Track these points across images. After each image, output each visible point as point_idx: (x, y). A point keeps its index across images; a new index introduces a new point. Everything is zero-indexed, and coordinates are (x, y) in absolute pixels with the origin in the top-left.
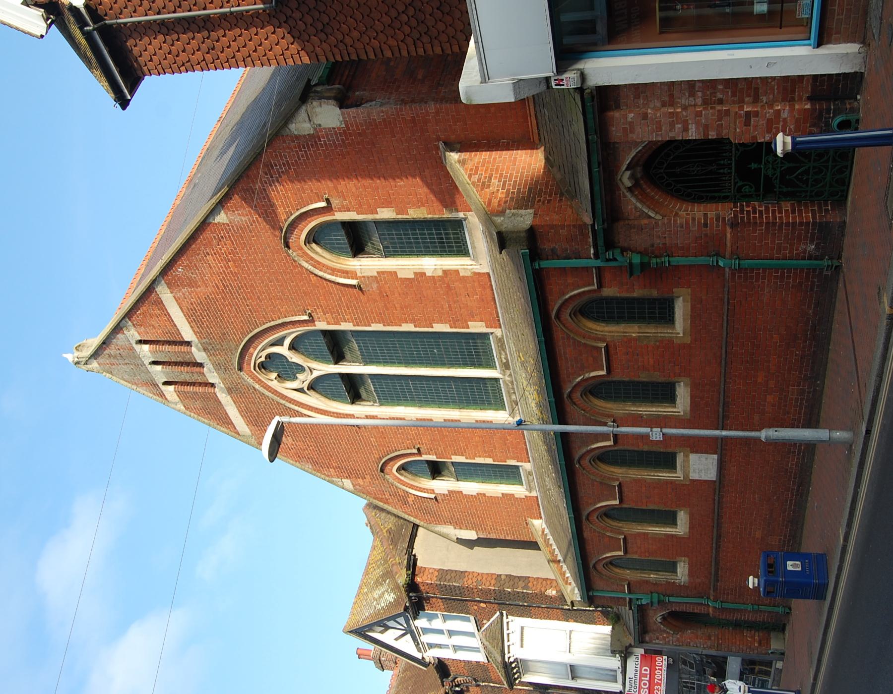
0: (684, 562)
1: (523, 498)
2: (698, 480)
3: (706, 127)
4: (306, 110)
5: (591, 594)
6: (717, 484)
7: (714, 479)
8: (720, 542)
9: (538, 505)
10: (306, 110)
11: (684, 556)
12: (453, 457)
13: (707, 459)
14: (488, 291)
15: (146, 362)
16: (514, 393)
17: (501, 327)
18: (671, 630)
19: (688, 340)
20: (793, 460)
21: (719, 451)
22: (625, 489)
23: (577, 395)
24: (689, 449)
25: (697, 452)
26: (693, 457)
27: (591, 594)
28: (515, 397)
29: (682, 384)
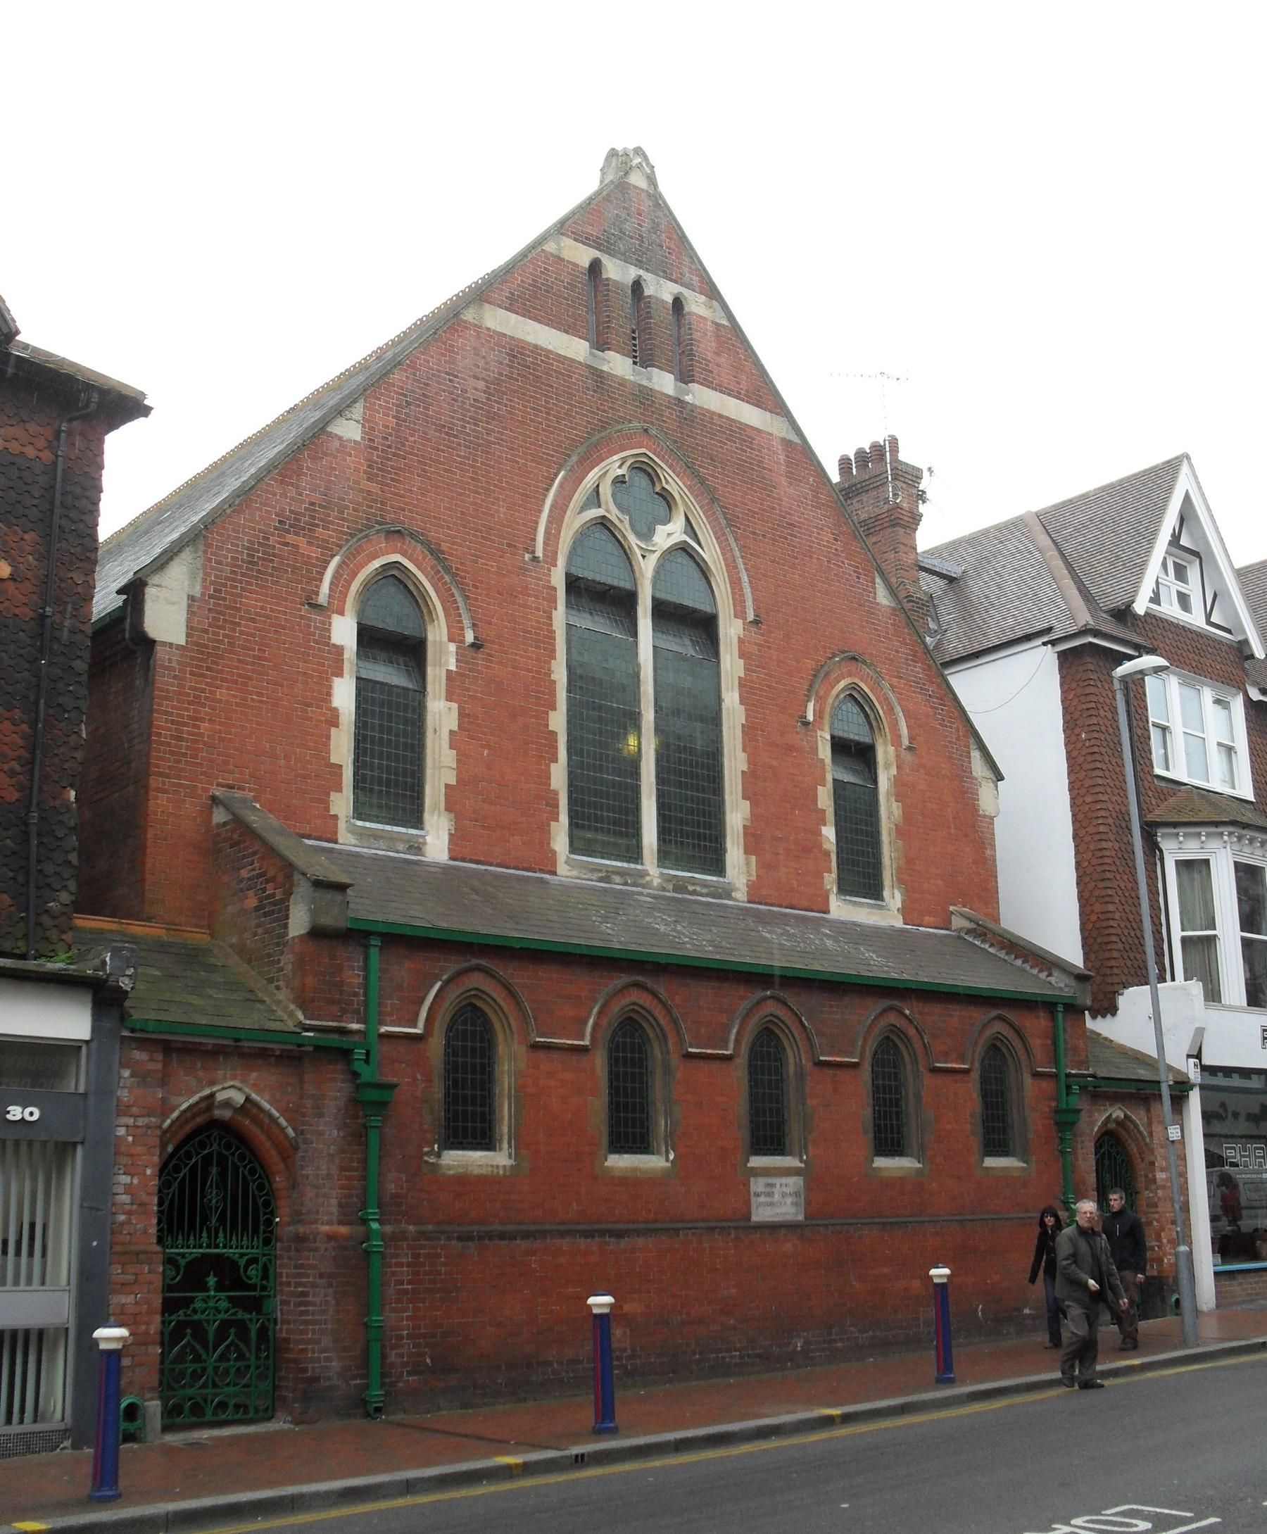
1: (327, 809)
3: (1164, 1187)
7: (755, 1218)
9: (463, 860)
12: (455, 706)
14: (805, 904)
15: (606, 260)
16: (626, 884)
17: (749, 902)
18: (173, 1123)
21: (809, 1222)
27: (375, 941)
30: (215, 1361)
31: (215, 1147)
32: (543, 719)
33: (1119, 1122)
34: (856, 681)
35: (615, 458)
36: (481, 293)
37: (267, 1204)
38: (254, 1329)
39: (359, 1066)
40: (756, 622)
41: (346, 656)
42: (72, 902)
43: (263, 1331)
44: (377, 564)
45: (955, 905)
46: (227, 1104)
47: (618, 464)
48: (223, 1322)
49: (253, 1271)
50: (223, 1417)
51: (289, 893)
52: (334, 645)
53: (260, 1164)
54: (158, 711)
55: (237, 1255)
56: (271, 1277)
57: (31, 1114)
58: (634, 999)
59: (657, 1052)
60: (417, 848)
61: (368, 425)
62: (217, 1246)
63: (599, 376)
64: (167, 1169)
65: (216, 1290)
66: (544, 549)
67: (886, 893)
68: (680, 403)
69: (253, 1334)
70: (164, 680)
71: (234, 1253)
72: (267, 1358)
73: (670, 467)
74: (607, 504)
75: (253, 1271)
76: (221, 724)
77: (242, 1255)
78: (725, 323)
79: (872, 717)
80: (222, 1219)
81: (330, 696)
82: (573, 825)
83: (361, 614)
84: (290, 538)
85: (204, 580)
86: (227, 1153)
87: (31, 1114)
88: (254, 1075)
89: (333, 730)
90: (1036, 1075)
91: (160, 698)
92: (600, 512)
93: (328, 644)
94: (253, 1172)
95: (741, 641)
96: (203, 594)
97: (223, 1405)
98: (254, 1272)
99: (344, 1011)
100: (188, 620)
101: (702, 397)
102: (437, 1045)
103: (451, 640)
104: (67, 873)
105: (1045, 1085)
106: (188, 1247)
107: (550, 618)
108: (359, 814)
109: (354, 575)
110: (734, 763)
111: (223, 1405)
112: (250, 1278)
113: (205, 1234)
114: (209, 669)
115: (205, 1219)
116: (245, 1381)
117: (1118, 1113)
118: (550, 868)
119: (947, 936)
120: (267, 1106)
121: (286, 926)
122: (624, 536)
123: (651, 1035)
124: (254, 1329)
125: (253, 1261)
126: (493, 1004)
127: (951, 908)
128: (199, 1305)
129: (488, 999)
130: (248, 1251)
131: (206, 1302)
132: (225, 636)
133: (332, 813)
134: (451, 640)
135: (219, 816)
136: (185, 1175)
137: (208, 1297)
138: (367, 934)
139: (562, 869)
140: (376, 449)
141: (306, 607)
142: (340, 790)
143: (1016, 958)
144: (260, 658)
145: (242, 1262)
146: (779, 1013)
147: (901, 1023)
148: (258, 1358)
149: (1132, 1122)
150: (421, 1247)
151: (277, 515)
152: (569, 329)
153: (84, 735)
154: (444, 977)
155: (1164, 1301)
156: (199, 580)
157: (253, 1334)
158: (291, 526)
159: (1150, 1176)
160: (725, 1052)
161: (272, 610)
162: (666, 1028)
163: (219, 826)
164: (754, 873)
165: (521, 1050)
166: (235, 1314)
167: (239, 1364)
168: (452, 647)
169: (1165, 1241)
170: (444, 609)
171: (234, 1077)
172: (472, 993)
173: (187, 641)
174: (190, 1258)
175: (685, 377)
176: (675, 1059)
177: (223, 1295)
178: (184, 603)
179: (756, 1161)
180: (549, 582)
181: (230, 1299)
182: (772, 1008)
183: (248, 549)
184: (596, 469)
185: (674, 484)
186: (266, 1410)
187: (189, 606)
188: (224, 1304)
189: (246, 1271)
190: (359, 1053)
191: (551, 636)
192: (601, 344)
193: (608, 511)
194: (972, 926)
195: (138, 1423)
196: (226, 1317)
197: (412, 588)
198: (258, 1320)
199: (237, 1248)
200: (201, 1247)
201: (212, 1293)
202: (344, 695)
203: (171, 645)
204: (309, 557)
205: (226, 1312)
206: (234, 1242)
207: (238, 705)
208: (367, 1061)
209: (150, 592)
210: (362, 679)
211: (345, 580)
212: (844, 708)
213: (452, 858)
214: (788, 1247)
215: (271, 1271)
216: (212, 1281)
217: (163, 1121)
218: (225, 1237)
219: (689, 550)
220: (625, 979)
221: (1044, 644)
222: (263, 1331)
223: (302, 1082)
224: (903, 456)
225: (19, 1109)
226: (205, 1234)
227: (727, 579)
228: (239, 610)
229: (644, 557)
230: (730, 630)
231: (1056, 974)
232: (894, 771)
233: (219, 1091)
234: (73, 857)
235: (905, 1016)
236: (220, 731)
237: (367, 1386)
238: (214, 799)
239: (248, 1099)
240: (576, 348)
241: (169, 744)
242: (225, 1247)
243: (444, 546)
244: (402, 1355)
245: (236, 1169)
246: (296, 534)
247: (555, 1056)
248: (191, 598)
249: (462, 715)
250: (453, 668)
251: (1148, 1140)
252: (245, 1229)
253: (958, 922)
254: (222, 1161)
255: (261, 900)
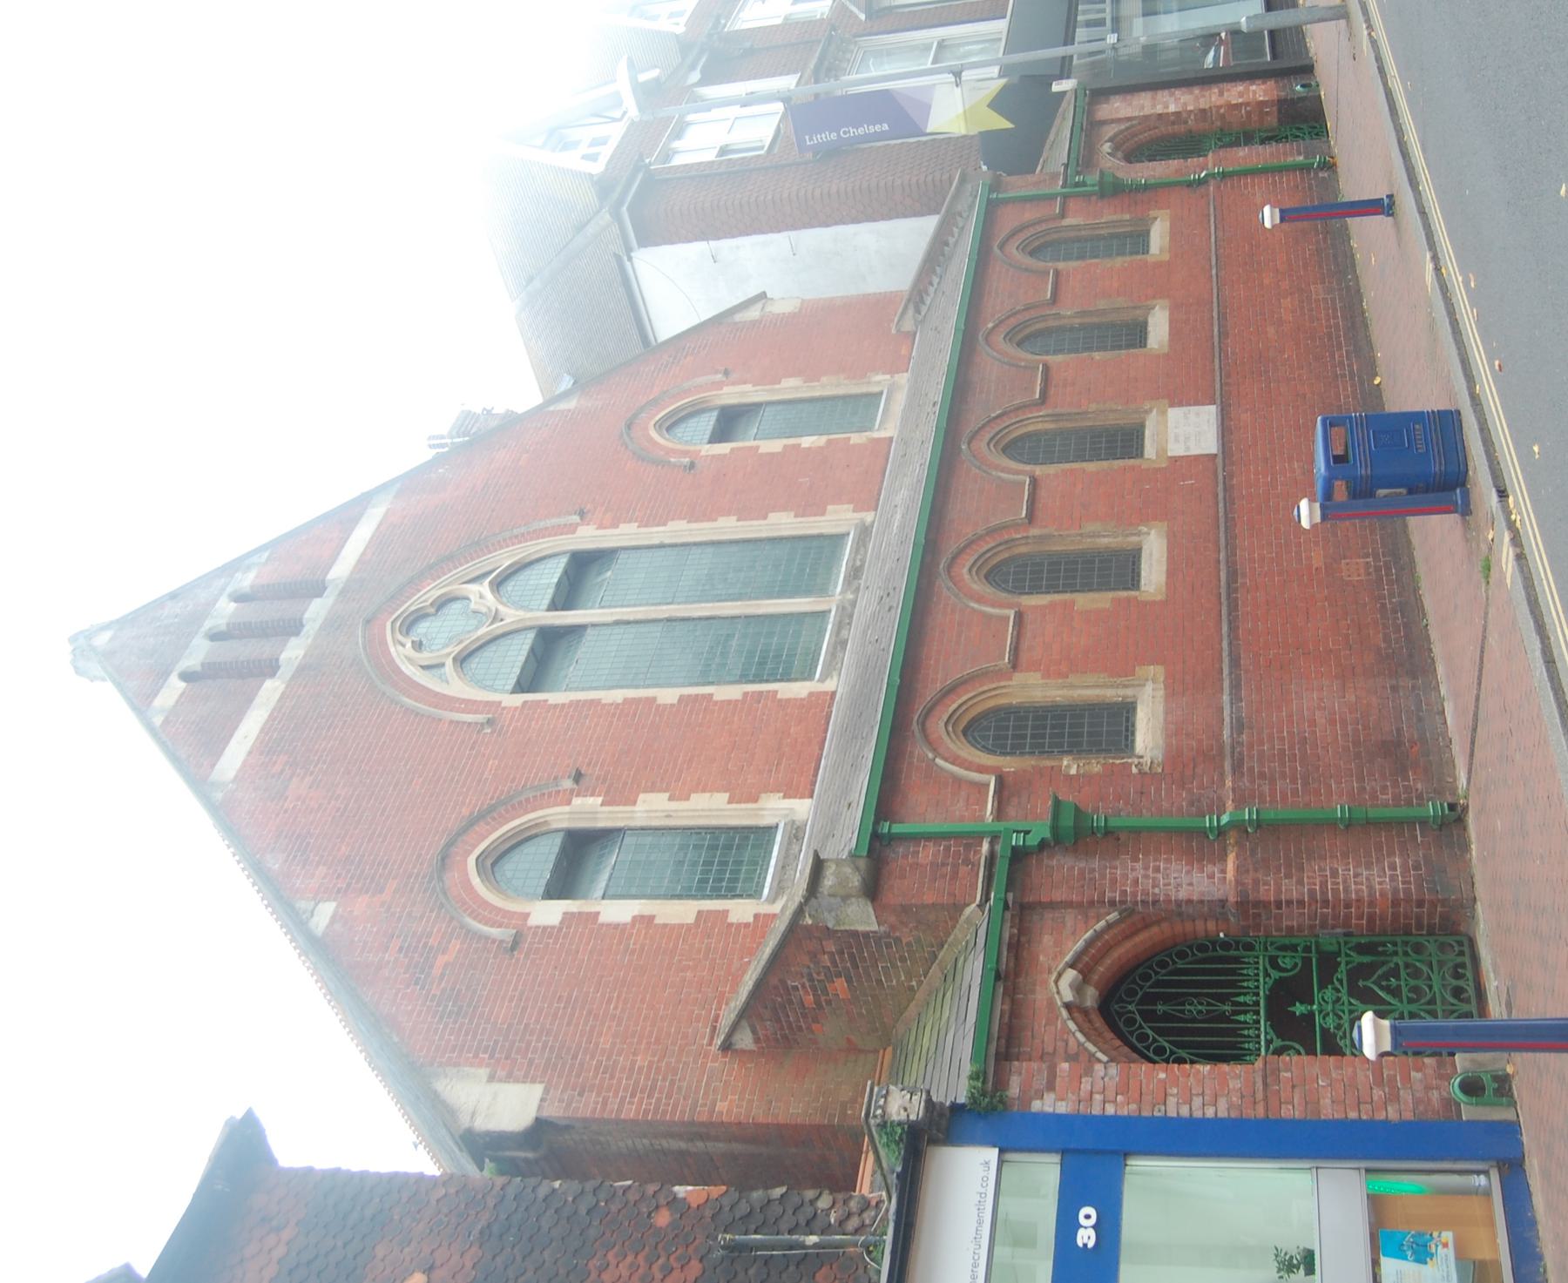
0: (1154, 681)
1: (747, 925)
2: (1183, 457)
4: (764, 305)
5: (885, 828)
6: (1220, 456)
8: (1236, 590)
10: (764, 305)
11: (1154, 662)
13: (1198, 414)
16: (850, 624)
17: (876, 510)
19: (1166, 257)
20: (1345, 389)
21: (1218, 401)
22: (1043, 493)
23: (999, 338)
24: (1166, 401)
25: (1180, 404)
26: (1175, 414)
27: (885, 828)
28: (846, 633)
29: (1157, 308)
30: (1401, 1001)
31: (1131, 1007)
32: (662, 710)
33: (1116, 148)
34: (653, 423)
35: (392, 650)
36: (199, 783)
37: (1202, 948)
38: (1358, 959)
39: (1033, 840)
40: (582, 514)
41: (575, 910)
42: (831, 1193)
43: (1361, 949)
44: (476, 881)
45: (890, 329)
46: (1078, 989)
47: (400, 648)
48: (1351, 994)
49: (1286, 961)
50: (1471, 992)
51: (829, 932)
52: (561, 923)
53: (1153, 957)
54: (619, 1110)
55: (1267, 979)
56: (1294, 941)
57: (1088, 1217)
58: (965, 570)
59: (1023, 549)
60: (796, 833)
61: (319, 896)
62: (1257, 1003)
63: (302, 670)
64: (1155, 1055)
65: (1312, 1003)
66: (481, 713)
67: (875, 389)
68: (344, 592)
69: (1366, 959)
70: (587, 1107)
71: (1265, 983)
72: (1395, 944)
73: (409, 598)
74: (441, 656)
75: (1286, 961)
76: (639, 1043)
77: (1267, 975)
78: (266, 554)
79: (690, 409)
80: (1223, 999)
81: (618, 925)
82: (786, 678)
83: (531, 897)
84: (436, 972)
85: (472, 1065)
86: (1140, 994)
87: (1088, 1217)
88: (1041, 958)
89: (657, 921)
90: (1063, 215)
91: (603, 1109)
92: (449, 662)
93: (560, 929)
94: (1163, 964)
95: (601, 527)
96: (488, 1065)
97: (1458, 992)
98: (1287, 960)
99: (967, 862)
100: (517, 1081)
101: (341, 570)
102: (1010, 764)
103: (569, 803)
104: (795, 1199)
105: (1071, 204)
106: (1258, 1036)
107: (556, 706)
108: (755, 894)
109: (486, 904)
110: (728, 527)
111: (1458, 992)
112: (1296, 965)
113: (1241, 1018)
114: (575, 1057)
115: (1223, 1017)
116: (1425, 968)
117: (1107, 147)
118: (828, 698)
119: (920, 337)
120: (1080, 944)
121: (866, 935)
122: (478, 639)
123: (1006, 555)
124: (1358, 959)
125: (1274, 963)
126: (964, 708)
127: (893, 331)
128: (1331, 1023)
129: (961, 711)
130: (1261, 968)
131: (1328, 1014)
132: (538, 1041)
133: (751, 920)
134: (569, 803)
135: (745, 1040)
136: (1167, 1041)
137: (1320, 1012)
138: (876, 836)
139: (830, 685)
140: (349, 885)
141: (516, 953)
142: (725, 913)
143: (943, 255)
144: (568, 1002)
145: (1275, 974)
146: (988, 437)
147: (1003, 330)
148: (1396, 953)
149: (1116, 135)
150: (1251, 769)
151: (408, 987)
152: (249, 700)
153: (629, 1182)
154: (930, 755)
155: (1301, 99)
156: (472, 1070)
157: (1366, 959)
158: (422, 972)
159: (1172, 118)
160: (1027, 483)
161: (515, 989)
162: (999, 540)
163: (757, 1040)
164: (846, 506)
165: (1018, 678)
166: (1341, 981)
167: (1403, 973)
168: (577, 801)
169: (1240, 100)
170: (533, 810)
171: (1045, 982)
172: (950, 729)
173: (541, 1082)
174: (1272, 1034)
175: (318, 589)
176: (1034, 532)
177: (1317, 996)
178: (496, 1086)
179: (1150, 451)
180: (516, 708)
181: (1322, 987)
182: (981, 444)
183: (441, 1018)
184: (403, 668)
185: (430, 592)
186: (1460, 944)
187: (500, 1081)
188: (1329, 993)
189: (1285, 970)
190: (1015, 840)
191: (576, 704)
192: (270, 668)
193: (449, 654)
194: (911, 307)
195: (1486, 1079)
196: (1344, 991)
197: (507, 845)
198: (1347, 955)
199: (1258, 981)
200: (1258, 1022)
201: (1315, 1007)
202: (618, 912)
203: (542, 1100)
204: (460, 951)
205: (1338, 991)
206: (1251, 984)
207: (619, 1025)
208: (1027, 833)
209: (482, 1124)
210: (604, 894)
211: (490, 913)
212: (679, 435)
213: (812, 797)
214: (1246, 417)
215: (1287, 941)
216: (1299, 1009)
217: (1099, 1061)
218: (1245, 994)
219: (499, 579)
220: (943, 584)
221: (630, 259)
222: (1361, 949)
223: (1053, 905)
224: (445, 432)
225: (1081, 1232)
226: (1241, 1018)
227: (534, 542)
228: (510, 1026)
229: (502, 620)
230: (588, 537)
231: (959, 207)
232: (748, 387)
233: (1061, 999)
234: (778, 1192)
235: (994, 328)
236: (648, 1043)
237: (1424, 822)
238: (727, 1047)
239: (1072, 965)
240: (271, 690)
241: (659, 1100)
242: (1257, 994)
243: (465, 811)
244: (1384, 788)
245: (1158, 984)
246: (431, 967)
247: (1025, 645)
248: (491, 1078)
249: (653, 789)
250: (600, 800)
251: (1134, 122)
252: (1233, 972)
253: (908, 325)
254: (1150, 999)
255: (839, 975)
